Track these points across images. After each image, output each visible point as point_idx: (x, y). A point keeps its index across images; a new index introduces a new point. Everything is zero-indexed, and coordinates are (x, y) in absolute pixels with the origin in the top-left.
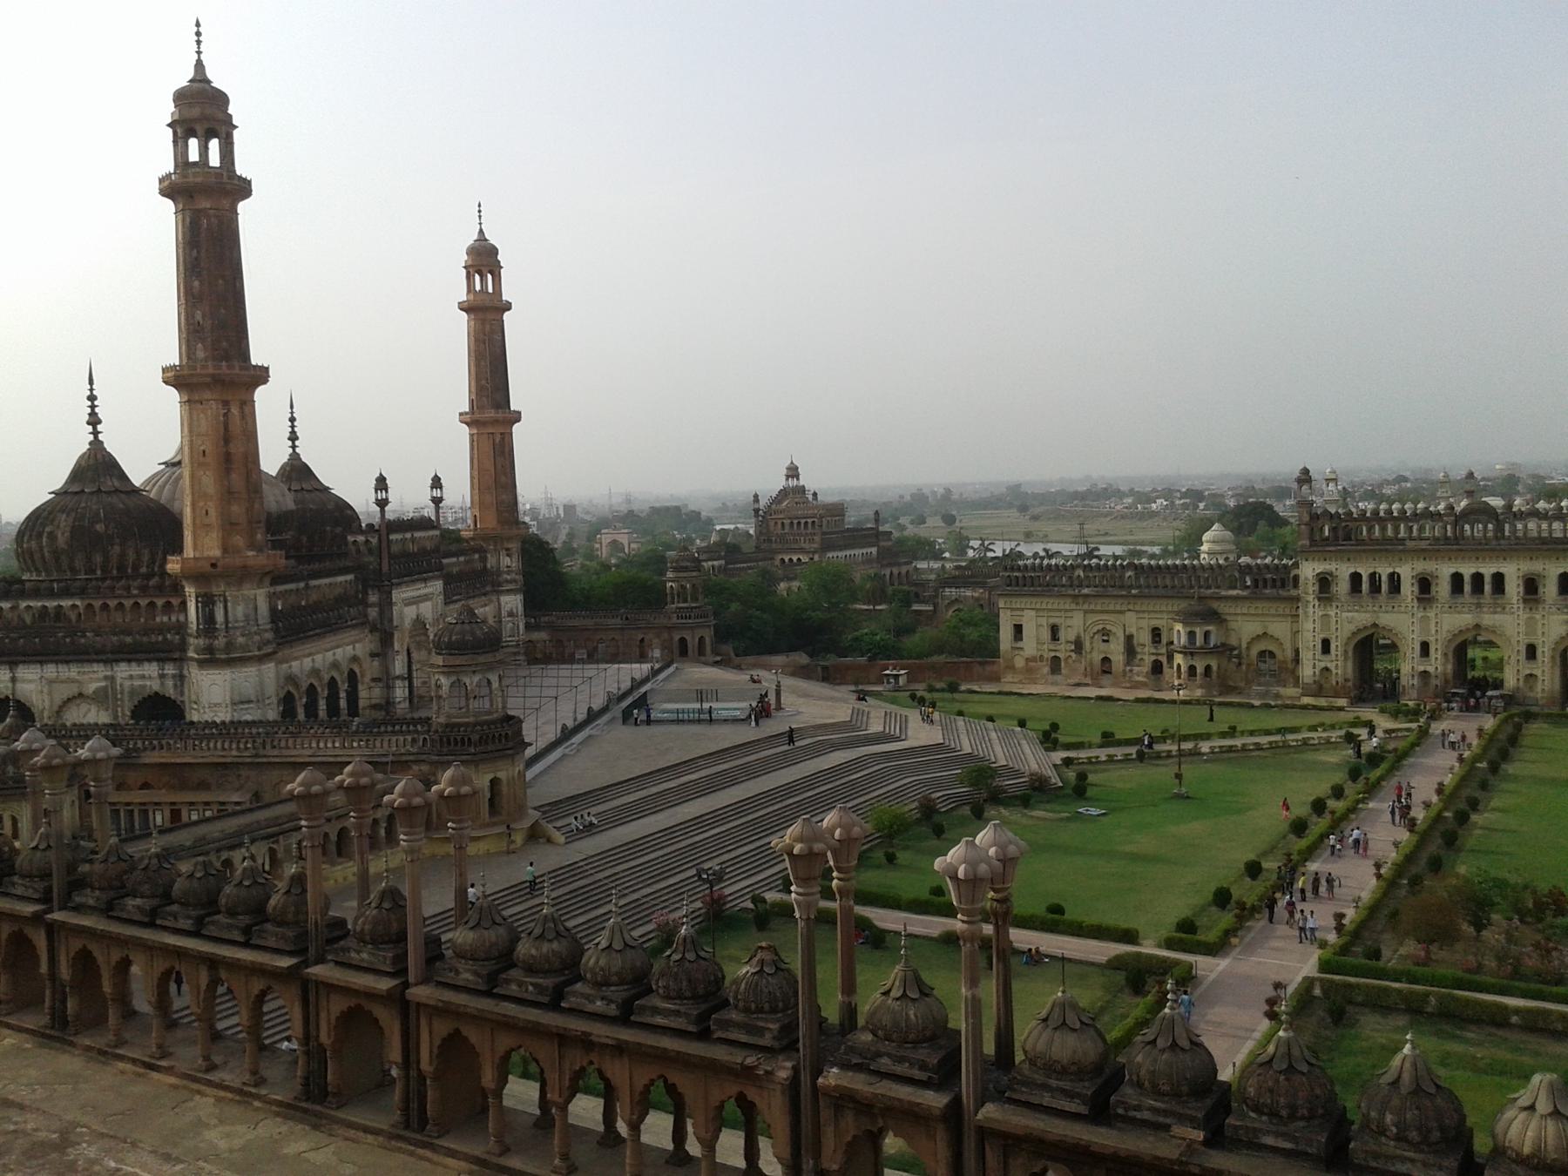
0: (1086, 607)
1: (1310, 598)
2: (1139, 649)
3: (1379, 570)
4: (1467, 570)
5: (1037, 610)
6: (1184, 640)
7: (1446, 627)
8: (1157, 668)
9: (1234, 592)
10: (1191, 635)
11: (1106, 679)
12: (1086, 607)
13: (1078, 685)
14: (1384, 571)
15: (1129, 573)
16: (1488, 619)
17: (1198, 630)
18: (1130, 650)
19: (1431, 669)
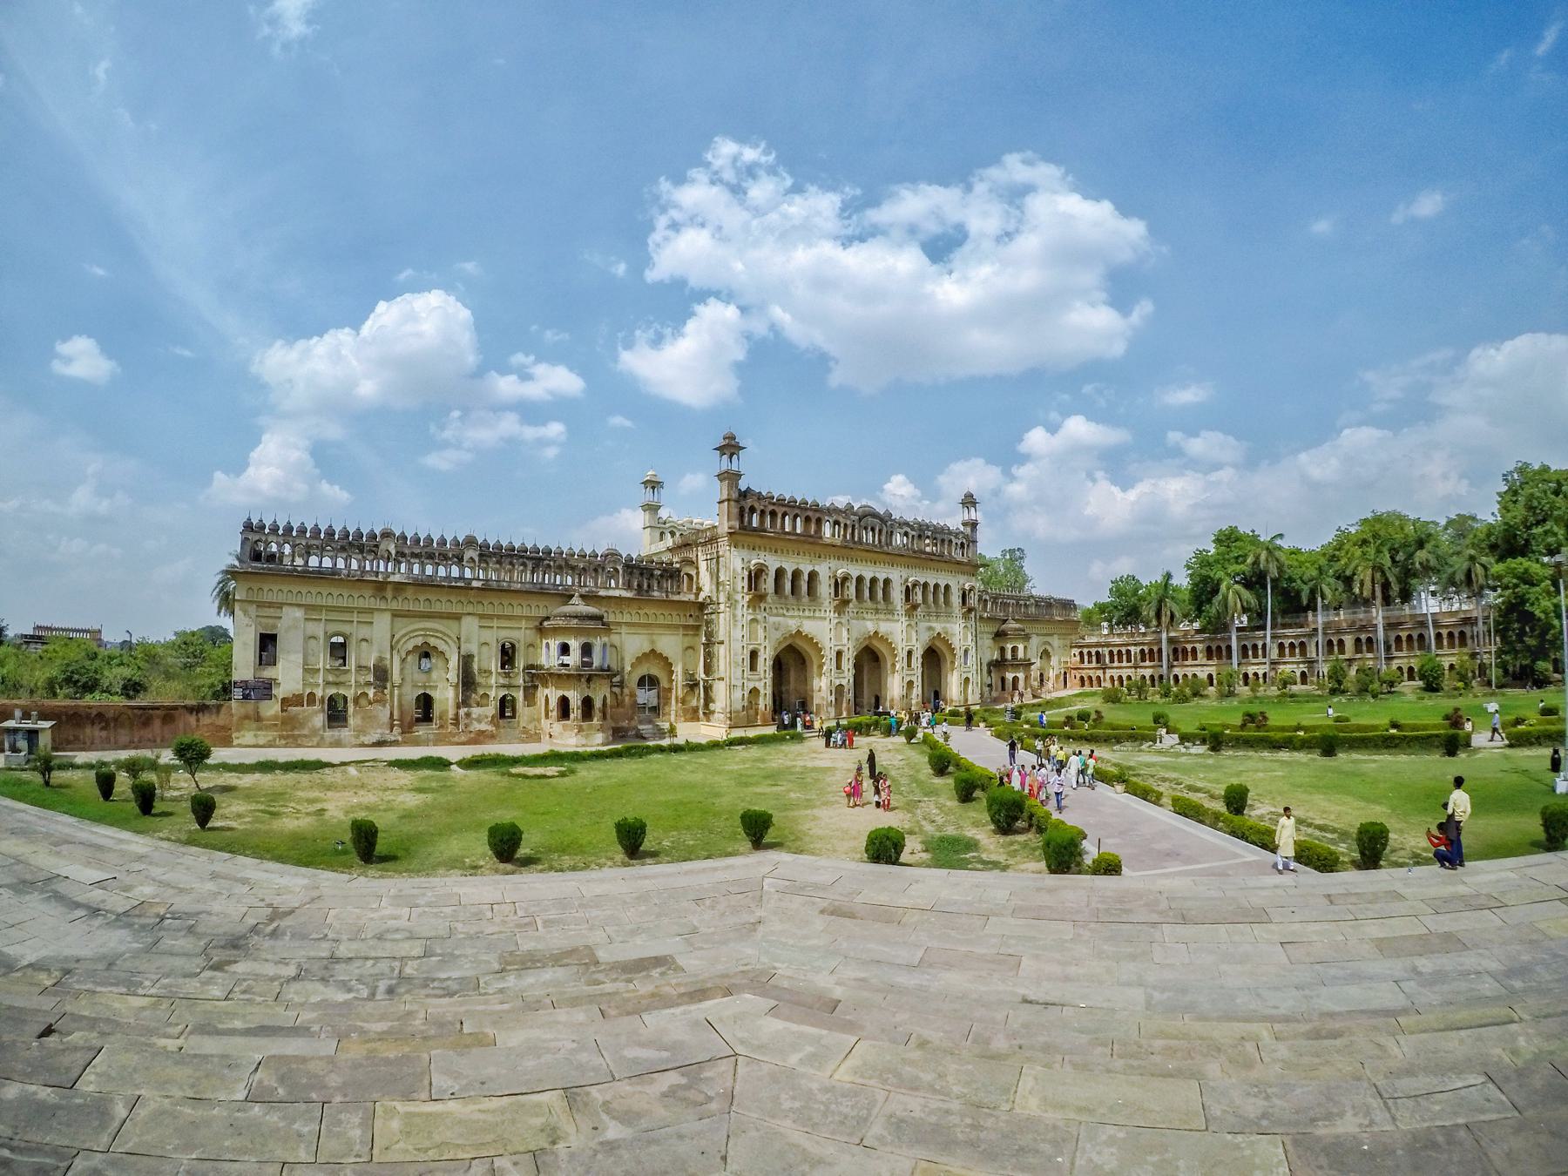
0: (394, 605)
1: (739, 597)
2: (479, 679)
3: (801, 567)
4: (868, 575)
5: (309, 608)
6: (574, 659)
7: (855, 634)
8: (506, 708)
9: (617, 593)
10: (587, 650)
11: (421, 731)
12: (394, 605)
13: (380, 744)
14: (806, 569)
15: (471, 553)
16: (884, 628)
17: (597, 644)
18: (468, 682)
19: (844, 682)
